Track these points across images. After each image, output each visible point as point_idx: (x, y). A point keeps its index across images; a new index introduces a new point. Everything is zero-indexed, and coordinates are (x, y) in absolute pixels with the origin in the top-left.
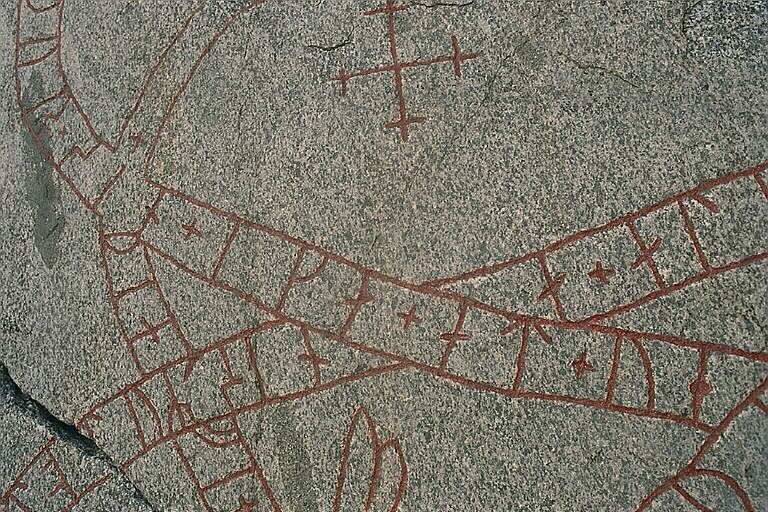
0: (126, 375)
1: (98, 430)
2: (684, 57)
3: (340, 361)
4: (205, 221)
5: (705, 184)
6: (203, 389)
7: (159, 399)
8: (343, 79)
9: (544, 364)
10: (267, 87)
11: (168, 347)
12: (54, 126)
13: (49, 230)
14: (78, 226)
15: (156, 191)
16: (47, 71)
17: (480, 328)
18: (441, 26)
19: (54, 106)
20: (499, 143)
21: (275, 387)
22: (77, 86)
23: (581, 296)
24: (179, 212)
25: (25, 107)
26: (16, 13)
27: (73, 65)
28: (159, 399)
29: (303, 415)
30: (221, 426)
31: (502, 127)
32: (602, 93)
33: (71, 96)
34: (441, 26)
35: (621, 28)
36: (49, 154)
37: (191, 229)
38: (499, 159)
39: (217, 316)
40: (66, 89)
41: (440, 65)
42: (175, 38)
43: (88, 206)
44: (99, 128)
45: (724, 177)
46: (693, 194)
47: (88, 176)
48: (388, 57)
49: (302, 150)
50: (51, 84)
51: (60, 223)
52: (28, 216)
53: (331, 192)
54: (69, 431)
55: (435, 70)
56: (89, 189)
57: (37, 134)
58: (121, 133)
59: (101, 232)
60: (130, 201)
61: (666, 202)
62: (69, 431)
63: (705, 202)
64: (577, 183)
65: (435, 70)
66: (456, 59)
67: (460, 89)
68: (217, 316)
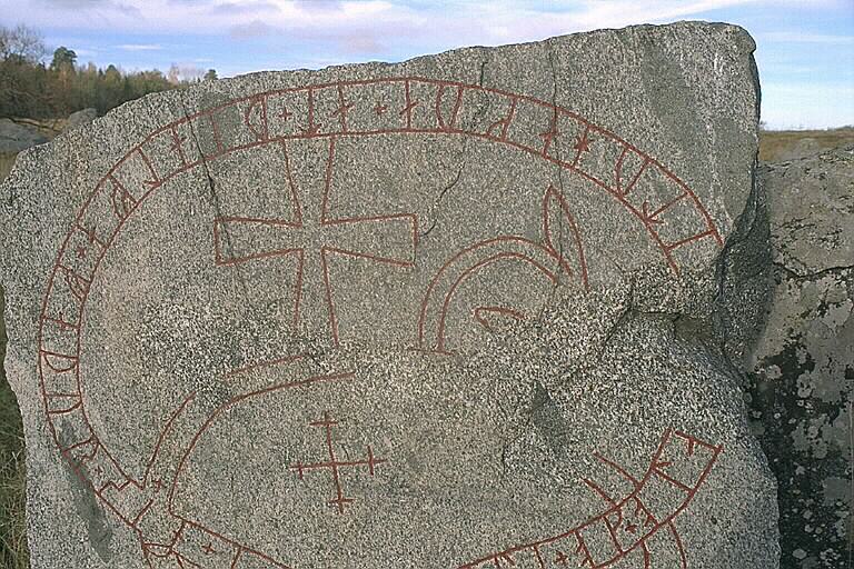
2: (502, 477)
4: (218, 545)
5: (509, 550)
8: (300, 468)
10: (249, 464)
12: (91, 466)
13: (101, 538)
14: (122, 537)
15: (179, 521)
16: (77, 423)
18: (361, 439)
19: (88, 450)
20: (397, 520)
22: (103, 436)
24: (197, 538)
26: (38, 370)
27: (96, 420)
31: (399, 510)
32: (457, 494)
33: (98, 443)
34: (361, 439)
35: (468, 457)
36: (89, 484)
37: (208, 548)
38: (398, 531)
40: (94, 439)
41: (361, 466)
42: (175, 415)
43: (129, 524)
44: (128, 471)
45: (518, 548)
46: (503, 554)
47: (125, 502)
48: (328, 456)
49: (277, 512)
51: (109, 534)
52: (81, 527)
53: (299, 539)
55: (358, 469)
57: (76, 468)
58: (145, 477)
59: (142, 543)
61: (489, 557)
63: (508, 559)
64: (441, 546)
65: (358, 469)
66: (371, 462)
67: (373, 485)
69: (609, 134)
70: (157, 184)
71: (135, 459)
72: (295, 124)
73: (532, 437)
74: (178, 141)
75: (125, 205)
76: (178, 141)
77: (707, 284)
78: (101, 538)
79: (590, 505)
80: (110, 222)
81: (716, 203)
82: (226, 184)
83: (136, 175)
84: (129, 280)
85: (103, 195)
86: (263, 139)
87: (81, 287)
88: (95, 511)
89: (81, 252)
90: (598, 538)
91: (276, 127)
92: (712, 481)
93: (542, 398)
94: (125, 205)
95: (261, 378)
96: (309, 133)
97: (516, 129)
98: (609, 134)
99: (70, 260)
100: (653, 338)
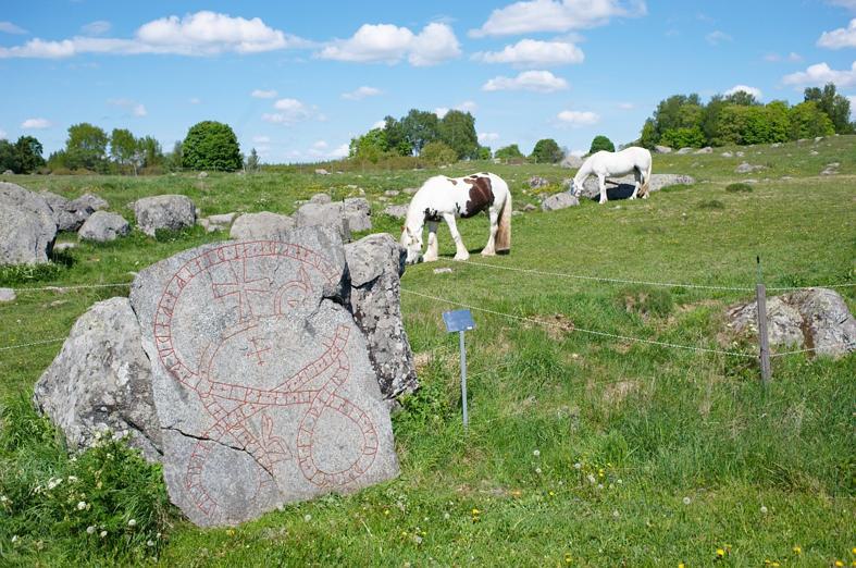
0: (214, 422)
1: (210, 435)
3: (258, 407)
6: (233, 419)
7: (223, 425)
9: (289, 399)
11: (222, 414)
13: (184, 398)
14: (192, 394)
17: (280, 396)
19: (177, 366)
21: (247, 415)
23: (293, 387)
24: (219, 387)
25: (168, 368)
27: (180, 356)
28: (223, 425)
29: (254, 418)
30: (238, 425)
39: (231, 405)
40: (179, 362)
47: (192, 382)
50: (174, 361)
52: (177, 395)
54: (200, 439)
56: (193, 385)
57: (173, 374)
60: (205, 387)
62: (200, 439)
68: (231, 405)
69: (312, 252)
70: (192, 276)
71: (195, 366)
72: (233, 256)
73: (307, 334)
74: (198, 263)
75: (182, 284)
76: (198, 263)
77: (340, 287)
78: (184, 398)
79: (324, 349)
80: (178, 290)
81: (338, 267)
82: (214, 274)
83: (185, 275)
84: (186, 308)
85: (174, 282)
86: (223, 260)
87: (169, 311)
88: (182, 388)
89: (168, 301)
90: (327, 358)
91: (227, 257)
92: (350, 337)
93: (307, 323)
94: (182, 284)
95: (233, 330)
96: (237, 258)
97: (290, 252)
98: (312, 252)
99: (164, 304)
100: (330, 303)
